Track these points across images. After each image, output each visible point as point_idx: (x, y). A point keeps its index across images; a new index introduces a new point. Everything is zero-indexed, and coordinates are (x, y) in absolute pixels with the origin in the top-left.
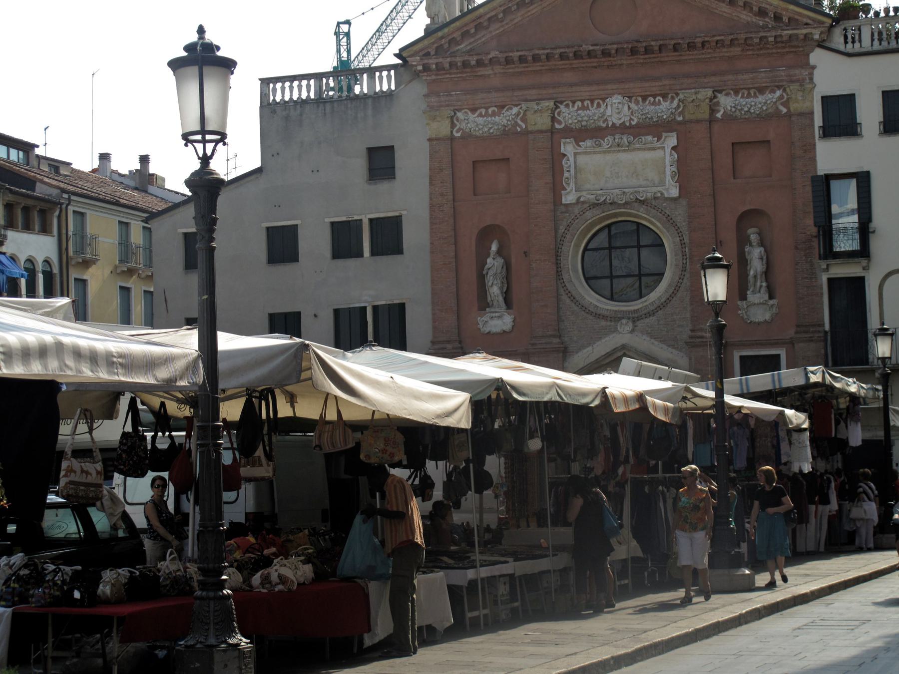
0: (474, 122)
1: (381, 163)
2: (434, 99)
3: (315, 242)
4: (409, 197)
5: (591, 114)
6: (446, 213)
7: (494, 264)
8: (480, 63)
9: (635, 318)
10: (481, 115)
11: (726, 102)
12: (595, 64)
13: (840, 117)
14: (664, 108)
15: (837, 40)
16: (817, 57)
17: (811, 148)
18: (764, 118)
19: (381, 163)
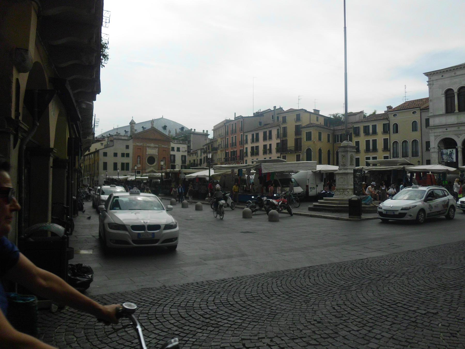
0: (138, 144)
1: (127, 147)
3: (119, 155)
4: (130, 151)
5: (150, 145)
9: (153, 167)
11: (163, 146)
13: (173, 149)
14: (157, 146)
16: (171, 143)
18: (166, 148)
19: (127, 147)
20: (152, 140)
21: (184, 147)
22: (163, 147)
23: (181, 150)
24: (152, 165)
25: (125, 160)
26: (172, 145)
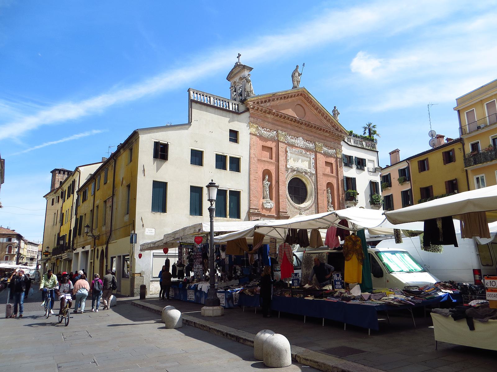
1: (234, 136)
2: (252, 119)
3: (209, 160)
8: (269, 113)
10: (264, 130)
12: (297, 125)
14: (311, 146)
19: (234, 136)
24: (302, 205)
25: (228, 181)
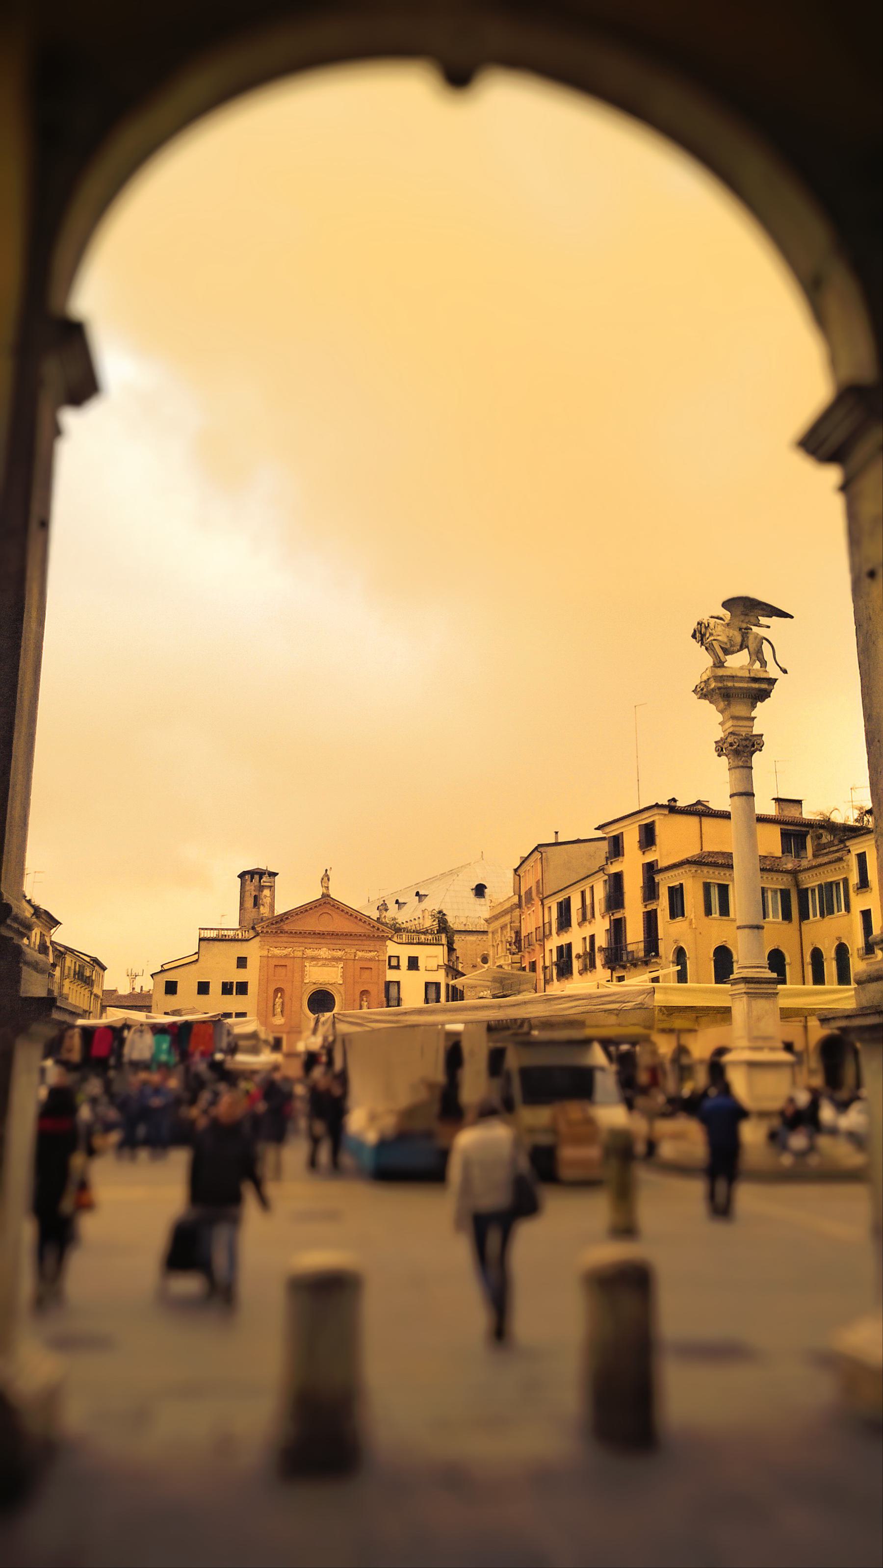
0: (277, 952)
1: (242, 962)
3: (215, 988)
5: (315, 953)
6: (264, 982)
7: (278, 1001)
14: (339, 954)
15: (395, 939)
16: (388, 942)
17: (385, 972)
19: (242, 962)
20: (321, 935)
21: (432, 957)
22: (361, 959)
23: (421, 963)
26: (392, 948)
